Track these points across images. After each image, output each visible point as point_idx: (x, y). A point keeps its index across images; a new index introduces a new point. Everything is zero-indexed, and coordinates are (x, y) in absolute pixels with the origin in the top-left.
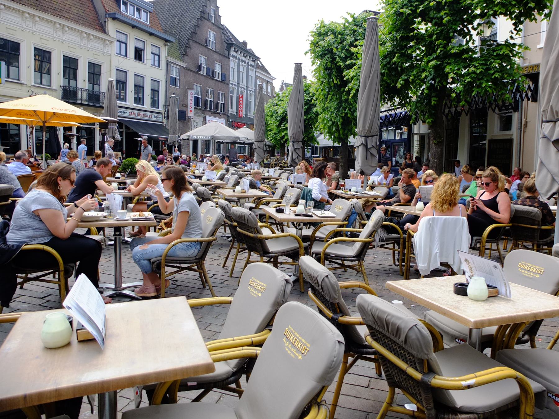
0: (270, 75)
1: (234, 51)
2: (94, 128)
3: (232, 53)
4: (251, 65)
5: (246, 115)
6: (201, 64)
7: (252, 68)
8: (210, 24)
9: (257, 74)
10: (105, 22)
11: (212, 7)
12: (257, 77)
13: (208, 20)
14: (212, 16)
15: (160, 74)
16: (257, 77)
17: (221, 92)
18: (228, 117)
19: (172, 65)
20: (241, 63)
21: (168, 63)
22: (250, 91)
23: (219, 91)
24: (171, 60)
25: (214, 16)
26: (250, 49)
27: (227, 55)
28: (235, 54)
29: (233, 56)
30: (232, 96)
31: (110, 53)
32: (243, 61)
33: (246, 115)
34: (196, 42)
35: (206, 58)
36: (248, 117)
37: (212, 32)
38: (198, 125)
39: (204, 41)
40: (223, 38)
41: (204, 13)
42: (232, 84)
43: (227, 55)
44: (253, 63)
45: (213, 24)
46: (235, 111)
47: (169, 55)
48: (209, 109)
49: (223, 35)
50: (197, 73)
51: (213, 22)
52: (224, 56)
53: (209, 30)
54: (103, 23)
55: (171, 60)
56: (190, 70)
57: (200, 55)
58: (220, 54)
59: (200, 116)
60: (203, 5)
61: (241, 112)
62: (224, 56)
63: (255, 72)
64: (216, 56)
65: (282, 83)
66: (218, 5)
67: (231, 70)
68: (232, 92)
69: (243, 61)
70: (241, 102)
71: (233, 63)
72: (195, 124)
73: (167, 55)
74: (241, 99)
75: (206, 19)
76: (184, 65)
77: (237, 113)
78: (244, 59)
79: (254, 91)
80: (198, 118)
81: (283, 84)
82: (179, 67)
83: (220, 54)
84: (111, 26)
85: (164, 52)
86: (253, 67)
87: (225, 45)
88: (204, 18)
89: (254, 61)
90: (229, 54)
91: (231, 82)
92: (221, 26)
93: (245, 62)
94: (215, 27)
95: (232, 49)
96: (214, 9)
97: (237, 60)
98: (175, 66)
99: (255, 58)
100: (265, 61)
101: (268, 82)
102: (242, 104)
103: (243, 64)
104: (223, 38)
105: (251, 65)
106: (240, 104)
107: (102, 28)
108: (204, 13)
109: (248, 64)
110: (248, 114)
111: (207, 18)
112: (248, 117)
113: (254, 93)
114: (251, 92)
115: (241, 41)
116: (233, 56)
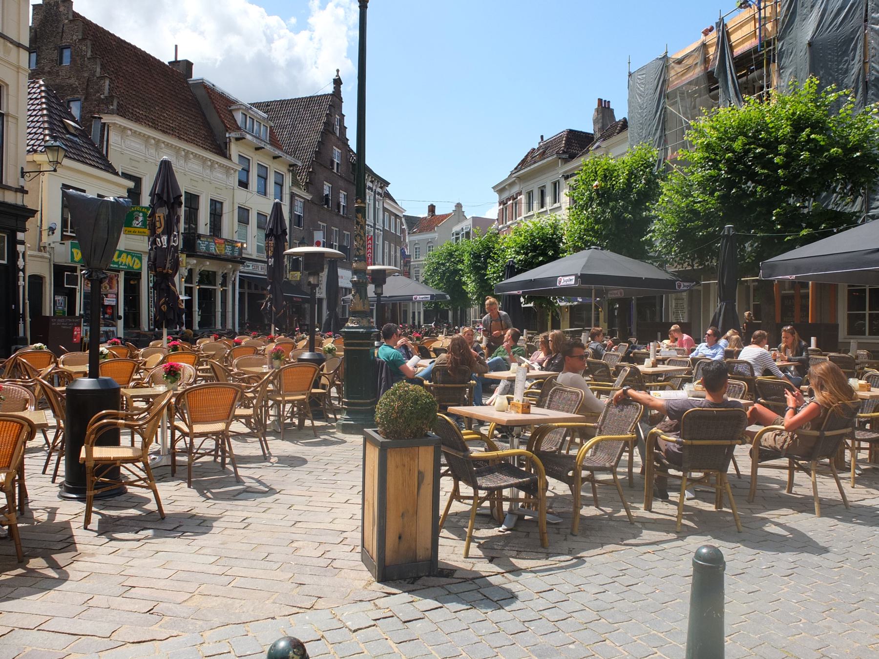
2: (215, 289)
4: (379, 194)
9: (386, 206)
10: (226, 143)
13: (334, 133)
16: (385, 210)
19: (296, 198)
22: (378, 229)
24: (296, 190)
35: (330, 185)
37: (337, 149)
39: (329, 163)
45: (338, 138)
52: (350, 182)
54: (223, 146)
62: (350, 182)
64: (341, 183)
75: (331, 133)
82: (303, 200)
83: (346, 180)
84: (235, 150)
88: (329, 131)
89: (381, 188)
94: (339, 143)
103: (370, 191)
107: (222, 150)
109: (375, 191)
114: (379, 231)
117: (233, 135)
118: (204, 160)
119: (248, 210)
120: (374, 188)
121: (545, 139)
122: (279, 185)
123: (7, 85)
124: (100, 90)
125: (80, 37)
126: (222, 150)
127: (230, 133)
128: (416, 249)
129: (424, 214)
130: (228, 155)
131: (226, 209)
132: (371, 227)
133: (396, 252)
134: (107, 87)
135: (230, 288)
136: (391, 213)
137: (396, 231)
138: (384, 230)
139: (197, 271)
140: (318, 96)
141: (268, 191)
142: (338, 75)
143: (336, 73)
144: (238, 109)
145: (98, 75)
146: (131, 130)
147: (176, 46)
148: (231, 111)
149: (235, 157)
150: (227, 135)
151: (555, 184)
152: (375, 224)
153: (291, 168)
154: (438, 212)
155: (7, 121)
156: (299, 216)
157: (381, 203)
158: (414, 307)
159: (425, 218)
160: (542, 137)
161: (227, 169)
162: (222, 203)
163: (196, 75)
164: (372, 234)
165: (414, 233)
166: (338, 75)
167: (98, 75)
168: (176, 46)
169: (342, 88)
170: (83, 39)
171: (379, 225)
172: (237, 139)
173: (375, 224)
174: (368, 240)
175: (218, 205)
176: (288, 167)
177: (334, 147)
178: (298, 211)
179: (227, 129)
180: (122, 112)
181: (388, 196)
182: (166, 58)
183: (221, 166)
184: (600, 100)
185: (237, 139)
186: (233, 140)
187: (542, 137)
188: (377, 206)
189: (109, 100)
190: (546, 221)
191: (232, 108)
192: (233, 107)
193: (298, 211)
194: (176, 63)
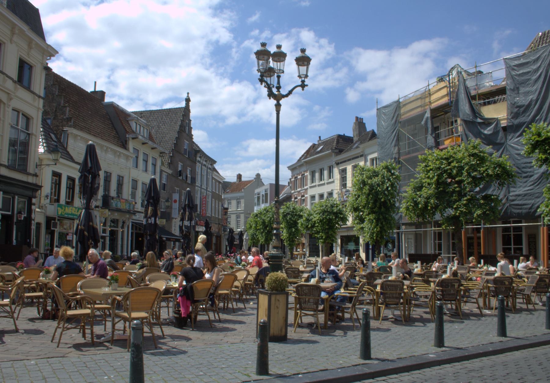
3: (198, 159)
4: (210, 169)
10: (126, 141)
16: (213, 178)
19: (164, 173)
20: (203, 167)
32: (205, 165)
35: (182, 164)
42: (197, 186)
44: (210, 166)
61: (204, 211)
69: (205, 165)
70: (204, 202)
71: (198, 166)
74: (204, 199)
78: (204, 163)
84: (131, 145)
89: (211, 165)
90: (196, 160)
93: (206, 166)
95: (199, 155)
102: (205, 204)
103: (204, 167)
105: (210, 169)
106: (203, 204)
107: (124, 145)
117: (131, 136)
118: (115, 152)
119: (137, 181)
120: (207, 165)
121: (322, 139)
122: (154, 165)
123: (33, 118)
124: (64, 113)
125: (52, 83)
126: (124, 145)
127: (129, 135)
129: (234, 179)
130: (127, 148)
131: (126, 181)
133: (219, 206)
134: (67, 112)
135: (126, 230)
136: (216, 181)
137: (219, 192)
138: (212, 192)
139: (109, 219)
140: (174, 109)
141: (148, 169)
142: (188, 96)
143: (187, 95)
144: (132, 120)
145: (62, 105)
146: (80, 136)
147: (95, 82)
148: (128, 121)
149: (131, 149)
150: (127, 136)
151: (330, 167)
152: (201, 185)
153: (161, 155)
154: (243, 179)
155: (32, 137)
156: (164, 184)
157: (211, 174)
159: (234, 183)
160: (320, 137)
161: (127, 158)
162: (123, 177)
163: (107, 100)
164: (205, 194)
165: (227, 192)
166: (188, 96)
167: (62, 105)
168: (95, 82)
169: (191, 104)
170: (54, 84)
171: (210, 189)
172: (133, 138)
173: (201, 185)
174: (203, 199)
175: (121, 178)
176: (159, 154)
177: (185, 140)
178: (164, 181)
179: (127, 132)
180: (75, 126)
181: (215, 170)
182: (90, 89)
183: (124, 154)
184: (357, 118)
185: (133, 138)
186: (131, 139)
187: (320, 137)
188: (203, 174)
189: (69, 119)
190: (325, 190)
192: (129, 118)
193: (164, 181)
194: (95, 92)
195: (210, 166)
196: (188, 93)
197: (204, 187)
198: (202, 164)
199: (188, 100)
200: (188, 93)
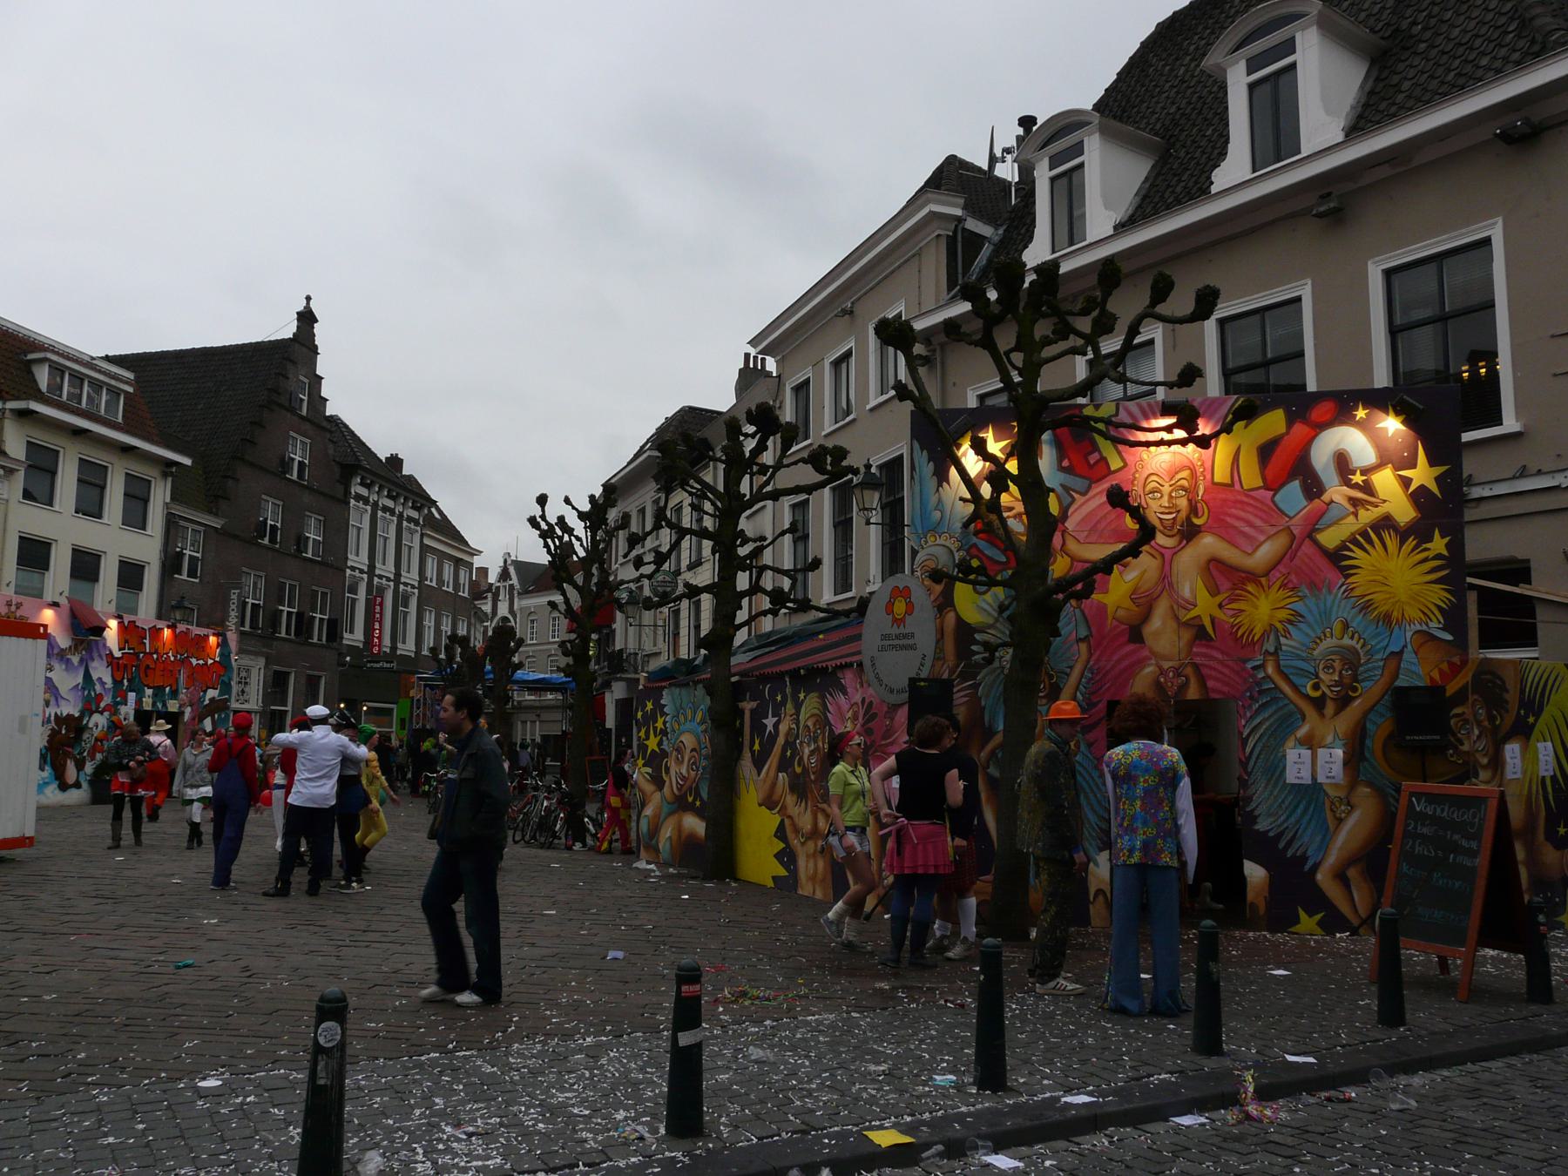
0: (466, 543)
1: (362, 484)
4: (410, 519)
5: (394, 648)
6: (266, 519)
7: (412, 526)
8: (296, 418)
9: (427, 541)
11: (302, 378)
12: (425, 549)
13: (293, 410)
14: (302, 400)
15: (147, 547)
17: (320, 590)
18: (340, 654)
19: (182, 523)
21: (171, 523)
23: (314, 588)
24: (179, 510)
25: (306, 398)
26: (411, 478)
27: (340, 495)
28: (364, 492)
29: (358, 497)
30: (354, 601)
31: (5, 497)
32: (385, 509)
33: (394, 648)
34: (252, 465)
36: (399, 652)
37: (300, 438)
38: (249, 676)
40: (331, 452)
41: (279, 394)
42: (353, 569)
43: (340, 495)
44: (415, 514)
45: (302, 417)
46: (362, 638)
47: (175, 497)
48: (283, 634)
49: (331, 446)
50: (253, 542)
51: (304, 412)
52: (333, 498)
53: (292, 433)
55: (179, 510)
56: (235, 537)
57: (264, 496)
58: (322, 493)
59: (256, 654)
60: (276, 374)
62: (333, 498)
63: (422, 535)
64: (307, 498)
65: (505, 561)
66: (318, 372)
67: (352, 533)
68: (354, 590)
72: (243, 674)
73: (168, 500)
75: (287, 410)
76: (216, 523)
77: (365, 643)
78: (390, 504)
79: (416, 584)
80: (252, 657)
81: (509, 562)
82: (202, 528)
83: (322, 493)
85: (160, 495)
86: (416, 522)
87: (337, 469)
90: (347, 492)
91: (350, 563)
92: (325, 424)
94: (307, 426)
96: (306, 381)
97: (369, 508)
98: (191, 526)
99: (421, 499)
100: (449, 504)
101: (458, 562)
104: (331, 452)
108: (279, 394)
109: (401, 515)
110: (400, 645)
111: (287, 404)
112: (399, 652)
113: (416, 591)
115: (383, 455)
116: (358, 497)
128: (532, 621)
132: (388, 579)
136: (442, 556)
157: (417, 538)
158: (524, 730)
171: (411, 576)
191: (31, 356)
195: (415, 514)
196: (308, 298)
197: (386, 568)
198: (375, 505)
199: (307, 318)
200: (308, 298)
